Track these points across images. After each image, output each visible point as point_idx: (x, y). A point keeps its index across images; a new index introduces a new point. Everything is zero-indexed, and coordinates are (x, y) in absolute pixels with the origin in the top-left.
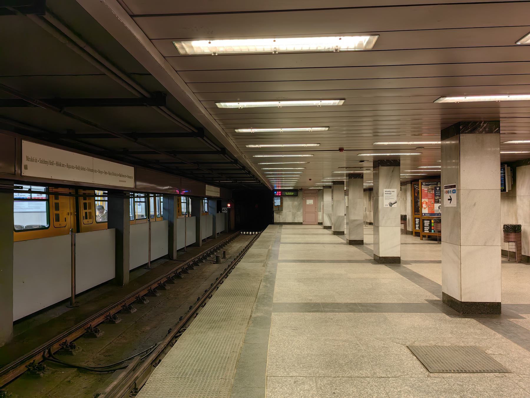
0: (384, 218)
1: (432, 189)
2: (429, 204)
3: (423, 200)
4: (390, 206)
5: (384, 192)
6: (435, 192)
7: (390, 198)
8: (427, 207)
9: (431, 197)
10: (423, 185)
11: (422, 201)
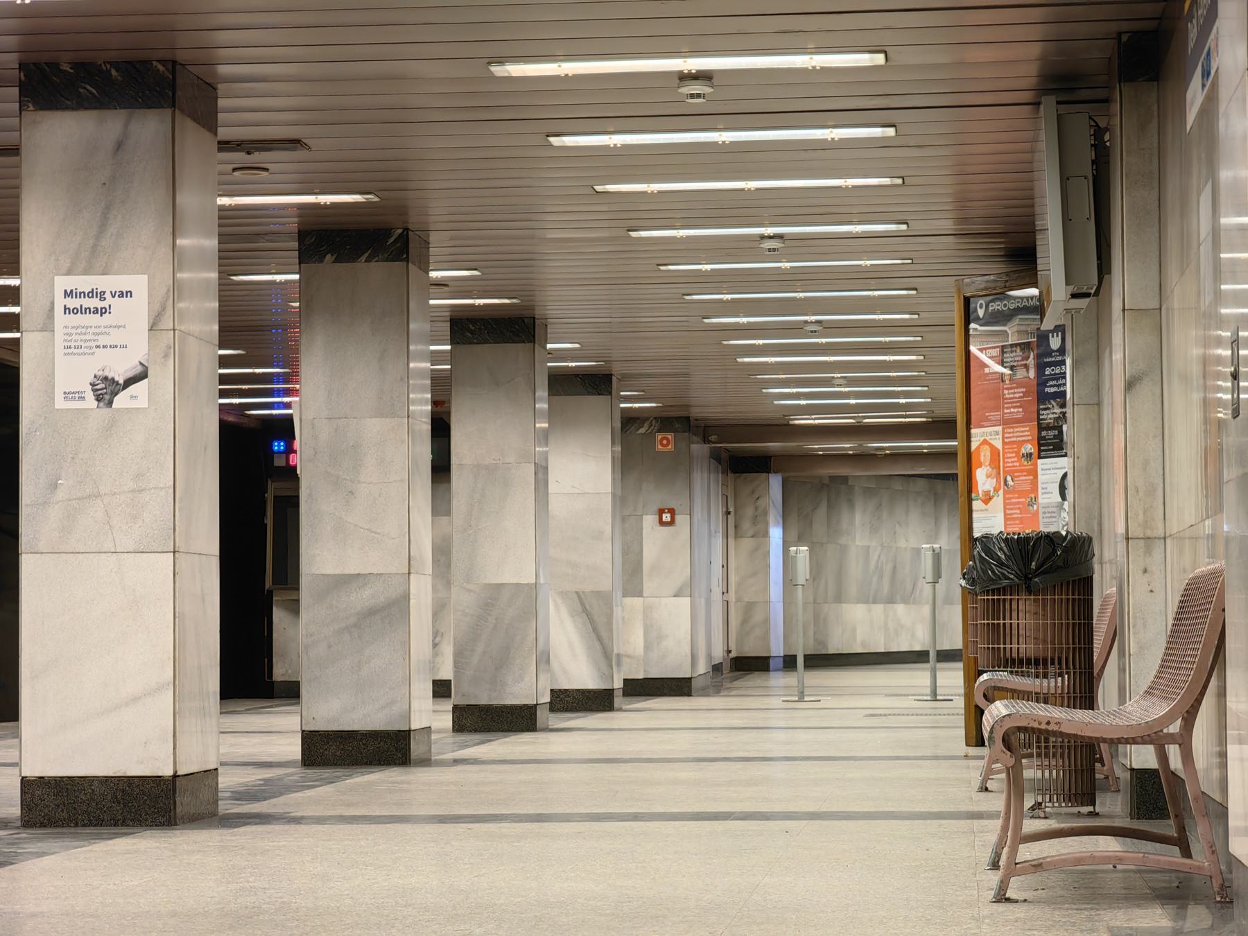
0: (54, 486)
1: (1025, 347)
2: (1012, 461)
3: (978, 435)
4: (99, 399)
5: (60, 302)
6: (1040, 367)
7: (103, 340)
8: (996, 490)
9: (1016, 412)
10: (977, 320)
11: (974, 446)
